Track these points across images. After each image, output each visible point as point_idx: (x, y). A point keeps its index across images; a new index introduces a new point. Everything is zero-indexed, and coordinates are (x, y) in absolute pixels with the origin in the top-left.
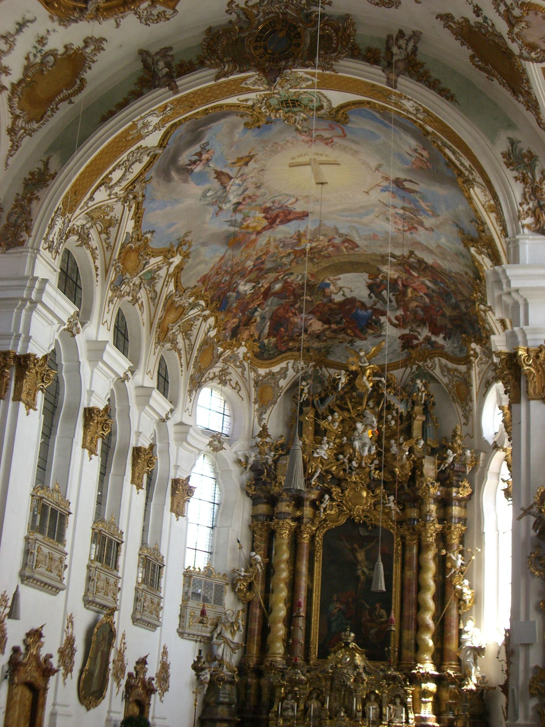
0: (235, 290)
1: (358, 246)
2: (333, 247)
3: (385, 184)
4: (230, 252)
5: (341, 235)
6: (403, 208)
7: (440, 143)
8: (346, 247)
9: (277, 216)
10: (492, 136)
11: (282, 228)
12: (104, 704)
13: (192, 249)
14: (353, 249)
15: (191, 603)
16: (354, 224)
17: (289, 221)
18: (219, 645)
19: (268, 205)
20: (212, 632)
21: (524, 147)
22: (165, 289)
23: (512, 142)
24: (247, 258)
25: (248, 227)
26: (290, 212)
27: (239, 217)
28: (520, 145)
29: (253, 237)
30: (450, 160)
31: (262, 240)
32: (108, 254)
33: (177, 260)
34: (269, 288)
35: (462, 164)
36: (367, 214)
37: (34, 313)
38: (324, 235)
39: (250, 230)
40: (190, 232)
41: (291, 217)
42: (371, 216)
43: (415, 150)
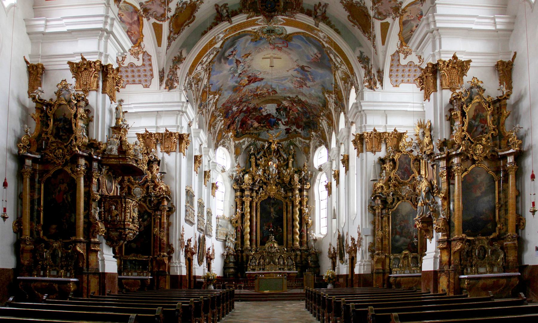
0: (231, 109)
1: (277, 93)
2: (268, 93)
3: (297, 68)
4: (233, 94)
5: (272, 88)
6: (300, 78)
7: (328, 52)
8: (272, 93)
9: (252, 79)
10: (354, 50)
11: (252, 85)
12: (202, 266)
13: (222, 92)
14: (275, 94)
15: (219, 228)
16: (279, 84)
17: (256, 82)
18: (229, 242)
19: (250, 75)
20: (226, 238)
21: (365, 54)
22: (212, 108)
23: (361, 53)
24: (238, 97)
25: (241, 84)
26: (257, 78)
27: (239, 79)
28: (364, 54)
29: (242, 88)
30: (331, 58)
31: (244, 89)
32: (198, 93)
33: (217, 97)
34: (242, 109)
35: (336, 61)
36: (285, 80)
37: (183, 117)
38: (266, 88)
39: (242, 85)
40: (223, 85)
41: (257, 80)
42: (287, 81)
43: (315, 54)
